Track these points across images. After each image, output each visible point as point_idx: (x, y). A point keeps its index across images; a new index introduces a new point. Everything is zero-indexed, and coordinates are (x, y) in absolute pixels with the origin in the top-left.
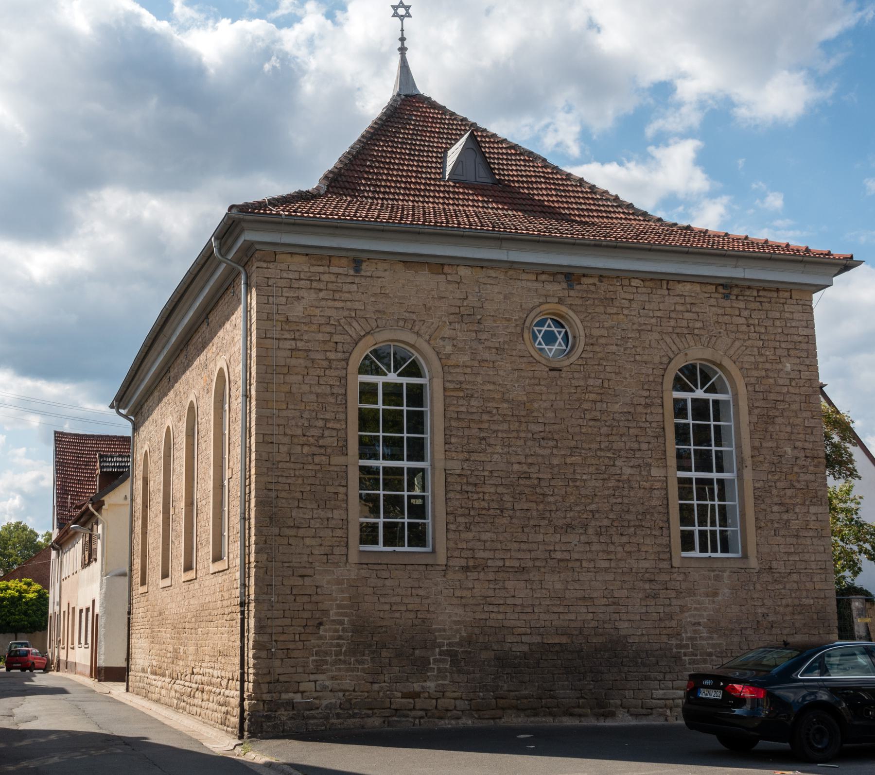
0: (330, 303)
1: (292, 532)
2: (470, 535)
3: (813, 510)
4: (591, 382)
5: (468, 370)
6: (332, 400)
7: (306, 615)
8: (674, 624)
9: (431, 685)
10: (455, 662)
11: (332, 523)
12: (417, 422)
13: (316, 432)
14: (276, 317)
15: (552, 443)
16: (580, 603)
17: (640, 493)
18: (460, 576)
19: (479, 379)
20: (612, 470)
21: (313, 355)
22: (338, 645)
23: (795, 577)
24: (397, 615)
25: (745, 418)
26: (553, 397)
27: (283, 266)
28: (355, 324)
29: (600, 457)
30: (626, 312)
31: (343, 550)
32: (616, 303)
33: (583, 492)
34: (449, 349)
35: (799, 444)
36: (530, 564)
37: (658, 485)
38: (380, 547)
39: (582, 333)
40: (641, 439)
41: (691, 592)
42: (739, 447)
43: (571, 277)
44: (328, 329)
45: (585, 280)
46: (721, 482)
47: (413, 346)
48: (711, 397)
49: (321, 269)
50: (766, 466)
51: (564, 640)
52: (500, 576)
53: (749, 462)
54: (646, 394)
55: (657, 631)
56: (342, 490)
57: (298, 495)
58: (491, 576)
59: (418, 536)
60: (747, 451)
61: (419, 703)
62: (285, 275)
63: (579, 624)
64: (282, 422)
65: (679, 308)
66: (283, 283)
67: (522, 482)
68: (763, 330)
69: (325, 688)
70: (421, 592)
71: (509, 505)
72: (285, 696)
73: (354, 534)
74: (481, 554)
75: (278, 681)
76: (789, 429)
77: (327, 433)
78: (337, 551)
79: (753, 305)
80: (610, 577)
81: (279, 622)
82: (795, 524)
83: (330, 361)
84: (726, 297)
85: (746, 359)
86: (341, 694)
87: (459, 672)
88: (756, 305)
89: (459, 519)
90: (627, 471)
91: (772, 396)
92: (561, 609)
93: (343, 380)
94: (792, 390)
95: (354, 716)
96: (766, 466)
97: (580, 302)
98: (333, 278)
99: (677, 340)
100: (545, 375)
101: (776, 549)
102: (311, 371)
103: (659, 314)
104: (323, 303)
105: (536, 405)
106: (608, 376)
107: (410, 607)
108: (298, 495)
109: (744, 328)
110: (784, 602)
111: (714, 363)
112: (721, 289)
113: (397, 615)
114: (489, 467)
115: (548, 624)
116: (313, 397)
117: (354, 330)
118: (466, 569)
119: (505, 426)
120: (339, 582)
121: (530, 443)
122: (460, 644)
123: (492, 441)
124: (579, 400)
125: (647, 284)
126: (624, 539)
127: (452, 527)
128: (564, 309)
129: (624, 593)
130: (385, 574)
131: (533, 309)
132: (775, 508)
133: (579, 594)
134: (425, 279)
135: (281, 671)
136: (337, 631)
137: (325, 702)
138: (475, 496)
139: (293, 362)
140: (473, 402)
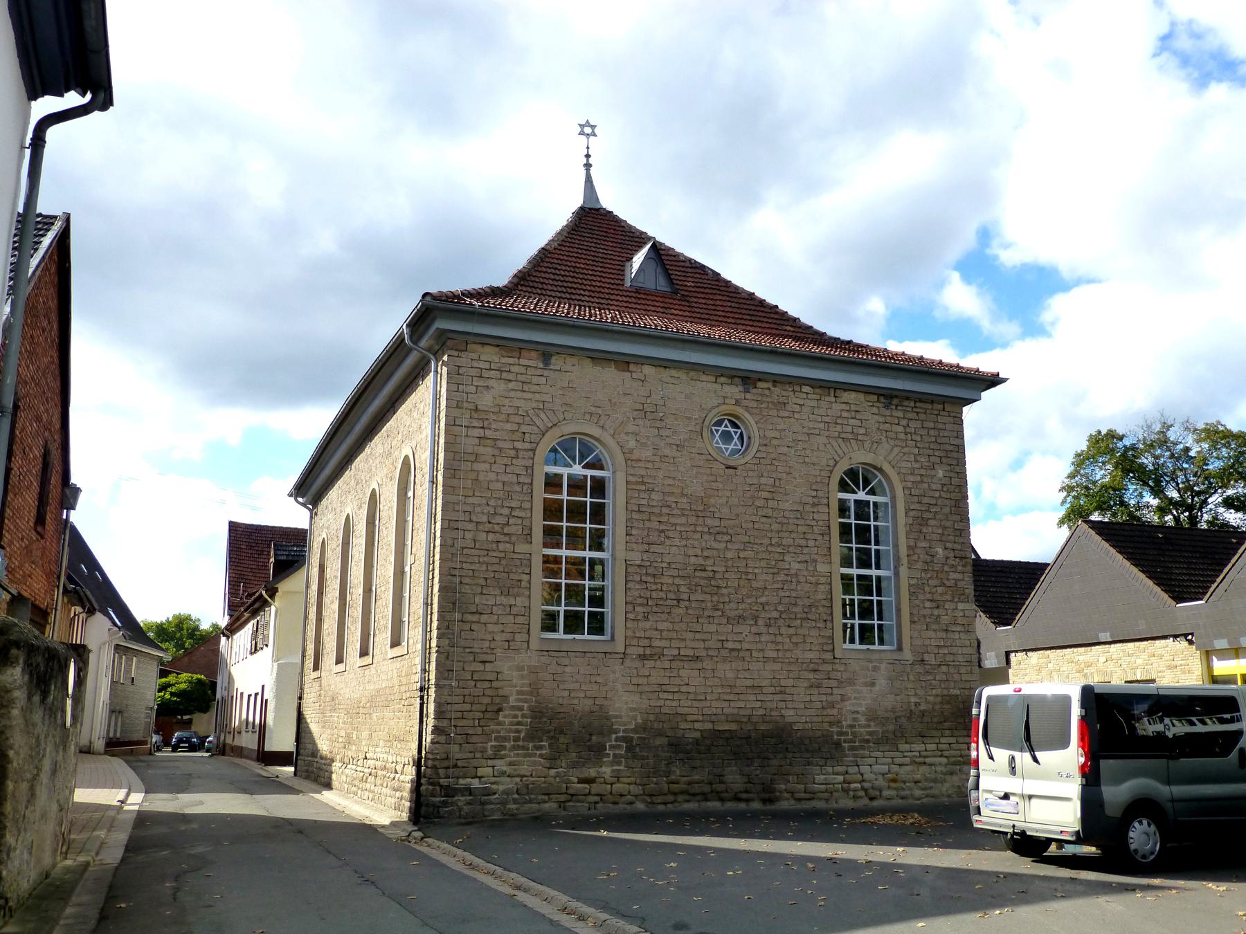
0: (519, 394)
1: (475, 618)
2: (647, 625)
3: (961, 606)
4: (764, 480)
5: (650, 465)
6: (518, 488)
7: (486, 700)
8: (835, 712)
9: (607, 771)
10: (629, 749)
11: (514, 610)
12: (599, 513)
13: (502, 520)
14: (465, 405)
15: (727, 538)
16: (749, 691)
17: (807, 587)
18: (638, 664)
19: (660, 474)
20: (781, 565)
21: (500, 444)
22: (518, 731)
23: (944, 669)
24: (576, 701)
25: (902, 520)
26: (728, 494)
27: (474, 356)
28: (543, 416)
29: (770, 552)
30: (797, 416)
31: (525, 637)
32: (789, 407)
33: (755, 585)
34: (632, 444)
35: (948, 545)
36: (703, 653)
37: (823, 580)
38: (560, 635)
39: (757, 435)
40: (808, 536)
41: (851, 682)
42: (896, 546)
43: (748, 380)
44: (517, 419)
45: (760, 384)
46: (879, 579)
47: (597, 439)
48: (872, 499)
49: (511, 361)
50: (919, 565)
51: (733, 727)
52: (674, 664)
53: (905, 560)
54: (814, 493)
55: (820, 719)
56: (525, 577)
57: (482, 582)
58: (667, 665)
59: (597, 624)
60: (903, 551)
61: (595, 788)
62: (475, 365)
63: (748, 712)
64: (469, 508)
65: (845, 414)
66: (473, 372)
67: (698, 574)
68: (918, 438)
69: (503, 773)
70: (599, 679)
71: (685, 596)
72: (461, 781)
73: (536, 621)
74: (657, 643)
75: (455, 766)
76: (940, 531)
77: (512, 521)
78: (518, 637)
79: (910, 415)
80: (777, 666)
81: (458, 707)
82: (945, 619)
83: (517, 450)
84: (887, 406)
85: (904, 464)
86: (518, 779)
87: (635, 757)
88: (914, 416)
89: (638, 609)
90: (795, 566)
91: (926, 500)
92: (731, 697)
93: (529, 469)
94: (944, 495)
95: (530, 801)
96: (919, 565)
97: (754, 404)
98: (523, 370)
99: (842, 445)
100: (722, 473)
101: (927, 642)
102: (498, 460)
103: (827, 419)
104: (512, 394)
105: (712, 501)
106: (780, 475)
107: (588, 694)
108: (482, 582)
109: (902, 436)
110: (934, 692)
111: (875, 468)
112: (882, 399)
113: (576, 701)
114: (667, 559)
115: (719, 711)
116: (500, 486)
117: (543, 420)
118: (643, 657)
119: (683, 520)
120: (520, 668)
121: (706, 537)
122: (635, 731)
123: (671, 534)
124: (753, 497)
125: (817, 390)
126: (792, 631)
127: (631, 616)
128: (740, 411)
129: (790, 682)
130: (566, 661)
131: (713, 408)
132: (928, 604)
133: (749, 683)
134: (610, 374)
135: (458, 756)
136: (516, 716)
137: (501, 788)
138: (654, 587)
139: (481, 450)
140: (654, 496)
